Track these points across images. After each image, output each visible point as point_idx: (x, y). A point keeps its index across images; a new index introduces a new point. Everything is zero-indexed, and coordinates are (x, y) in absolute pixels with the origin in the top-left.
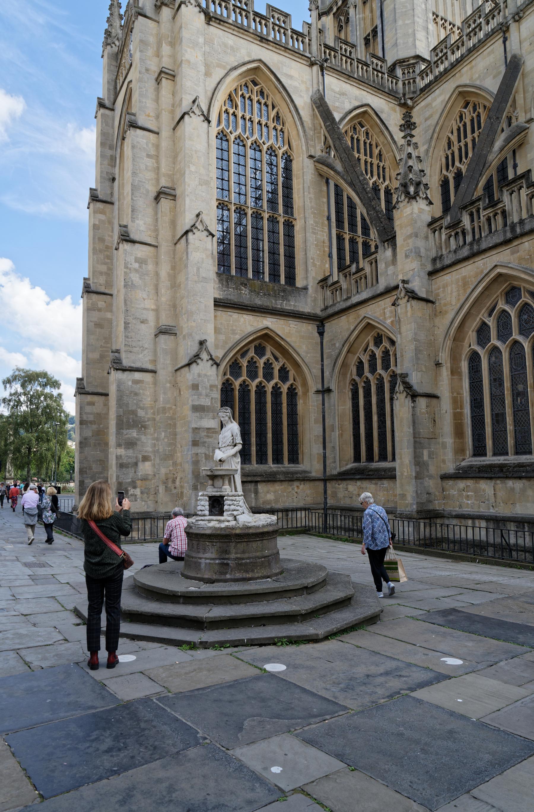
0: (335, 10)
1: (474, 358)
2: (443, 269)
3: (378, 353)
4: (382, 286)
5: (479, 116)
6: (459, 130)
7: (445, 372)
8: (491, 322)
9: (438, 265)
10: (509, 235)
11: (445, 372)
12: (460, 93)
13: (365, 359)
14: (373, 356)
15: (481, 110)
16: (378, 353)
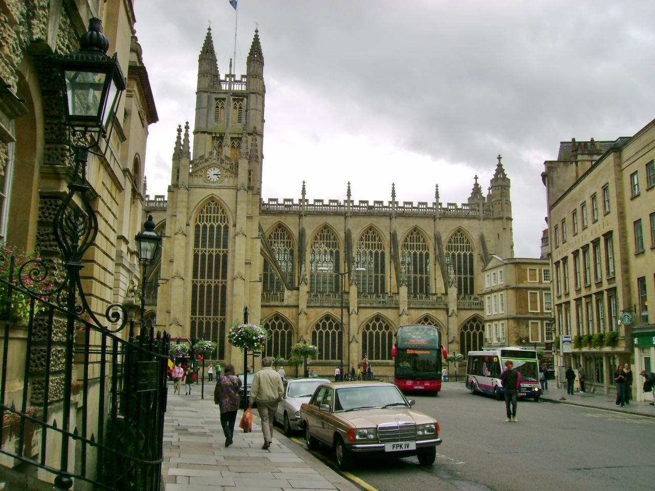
0: (214, 135)
1: (314, 333)
2: (311, 307)
3: (277, 323)
4: (285, 303)
5: (284, 234)
6: (275, 234)
7: (308, 335)
8: (321, 324)
9: (309, 305)
10: (332, 305)
11: (308, 335)
12: (280, 224)
13: (270, 324)
14: (273, 324)
15: (285, 233)
16: (277, 323)
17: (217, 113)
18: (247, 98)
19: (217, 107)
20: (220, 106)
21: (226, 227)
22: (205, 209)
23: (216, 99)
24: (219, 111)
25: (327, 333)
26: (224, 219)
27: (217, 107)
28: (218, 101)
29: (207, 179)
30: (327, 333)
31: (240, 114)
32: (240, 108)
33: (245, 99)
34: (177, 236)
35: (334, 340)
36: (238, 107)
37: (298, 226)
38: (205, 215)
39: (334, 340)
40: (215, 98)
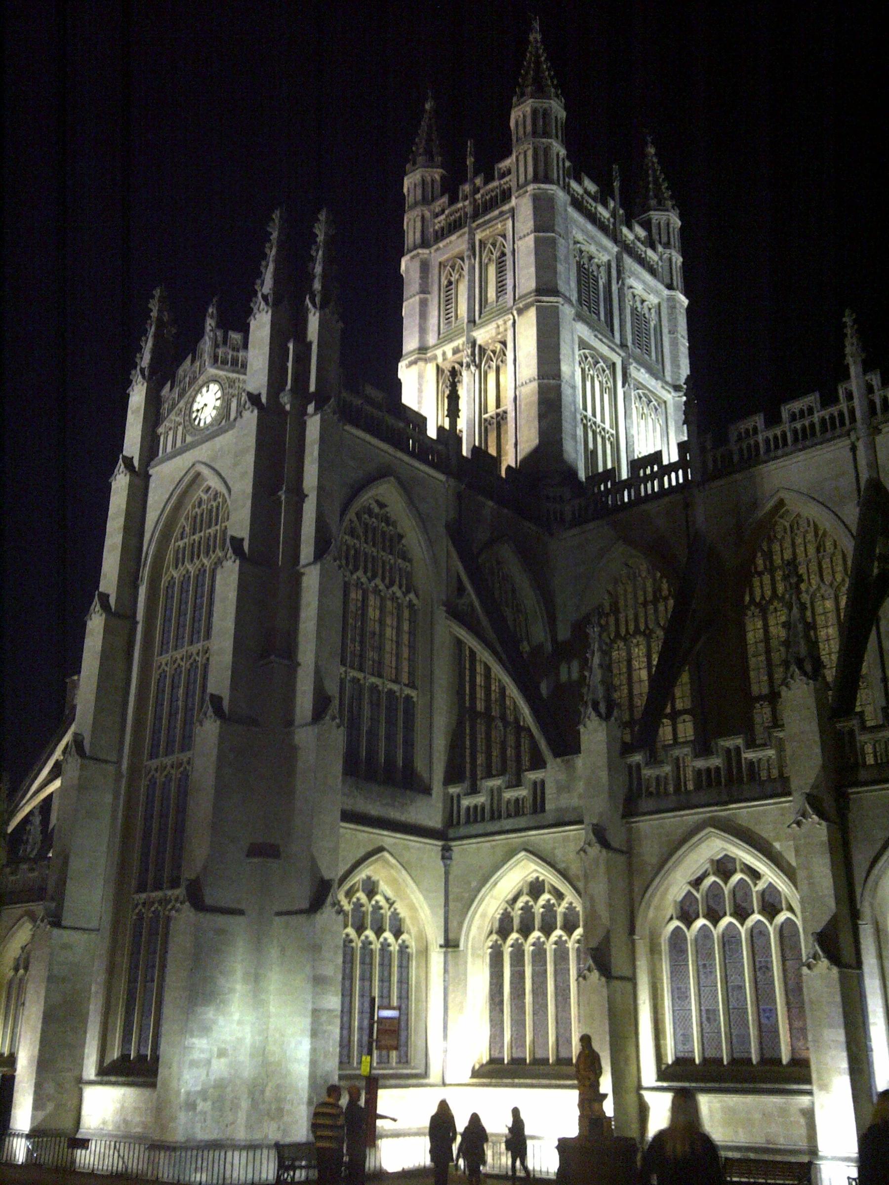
32: (503, 254)
35: (761, 968)
39: (761, 968)
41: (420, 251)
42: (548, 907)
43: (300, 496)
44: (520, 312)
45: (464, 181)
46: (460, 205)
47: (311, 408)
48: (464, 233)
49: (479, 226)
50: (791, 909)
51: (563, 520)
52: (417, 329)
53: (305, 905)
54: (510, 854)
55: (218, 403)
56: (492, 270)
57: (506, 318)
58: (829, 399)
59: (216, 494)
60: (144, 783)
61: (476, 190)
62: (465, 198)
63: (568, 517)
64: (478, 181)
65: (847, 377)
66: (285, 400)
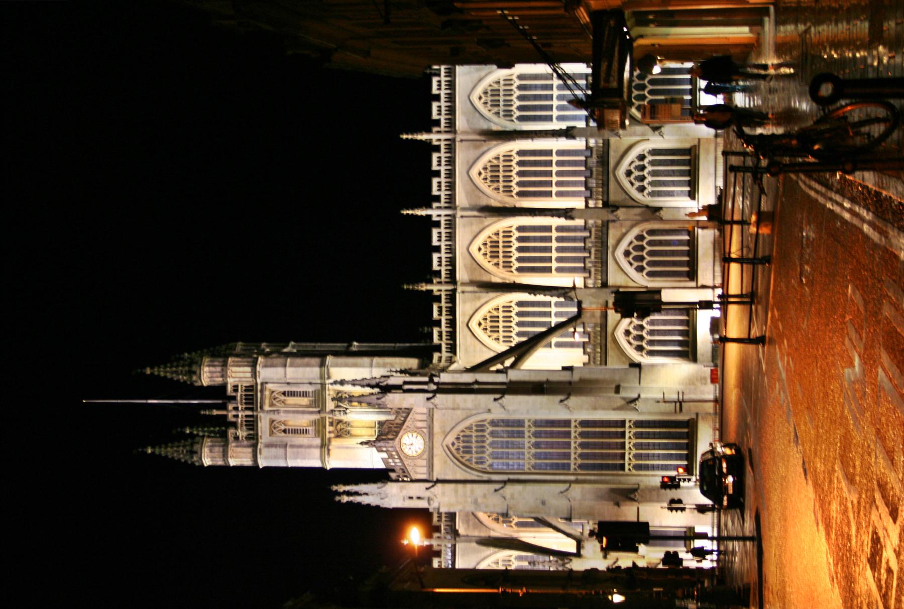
13: (636, 343)
17: (295, 432)
18: (267, 383)
19: (285, 431)
20: (283, 427)
21: (493, 423)
22: (465, 455)
23: (272, 433)
24: (290, 428)
25: (651, 253)
26: (480, 428)
27: (285, 431)
28: (275, 431)
29: (419, 457)
30: (651, 253)
31: (292, 394)
32: (284, 393)
33: (269, 386)
34: (508, 496)
36: (283, 398)
37: (477, 294)
38: (474, 455)
40: (270, 435)
41: (259, 447)
42: (635, 328)
43: (477, 382)
44: (329, 378)
45: (225, 416)
46: (239, 420)
47: (436, 380)
48: (261, 417)
49: (261, 408)
50: (642, 231)
51: (451, 357)
52: (308, 450)
53: (637, 370)
54: (615, 341)
55: (415, 435)
56: (291, 400)
57: (327, 388)
58: (437, 224)
59: (458, 439)
60: (579, 471)
61: (236, 409)
62: (236, 416)
63: (449, 355)
64: (230, 407)
65: (430, 216)
66: (433, 387)
